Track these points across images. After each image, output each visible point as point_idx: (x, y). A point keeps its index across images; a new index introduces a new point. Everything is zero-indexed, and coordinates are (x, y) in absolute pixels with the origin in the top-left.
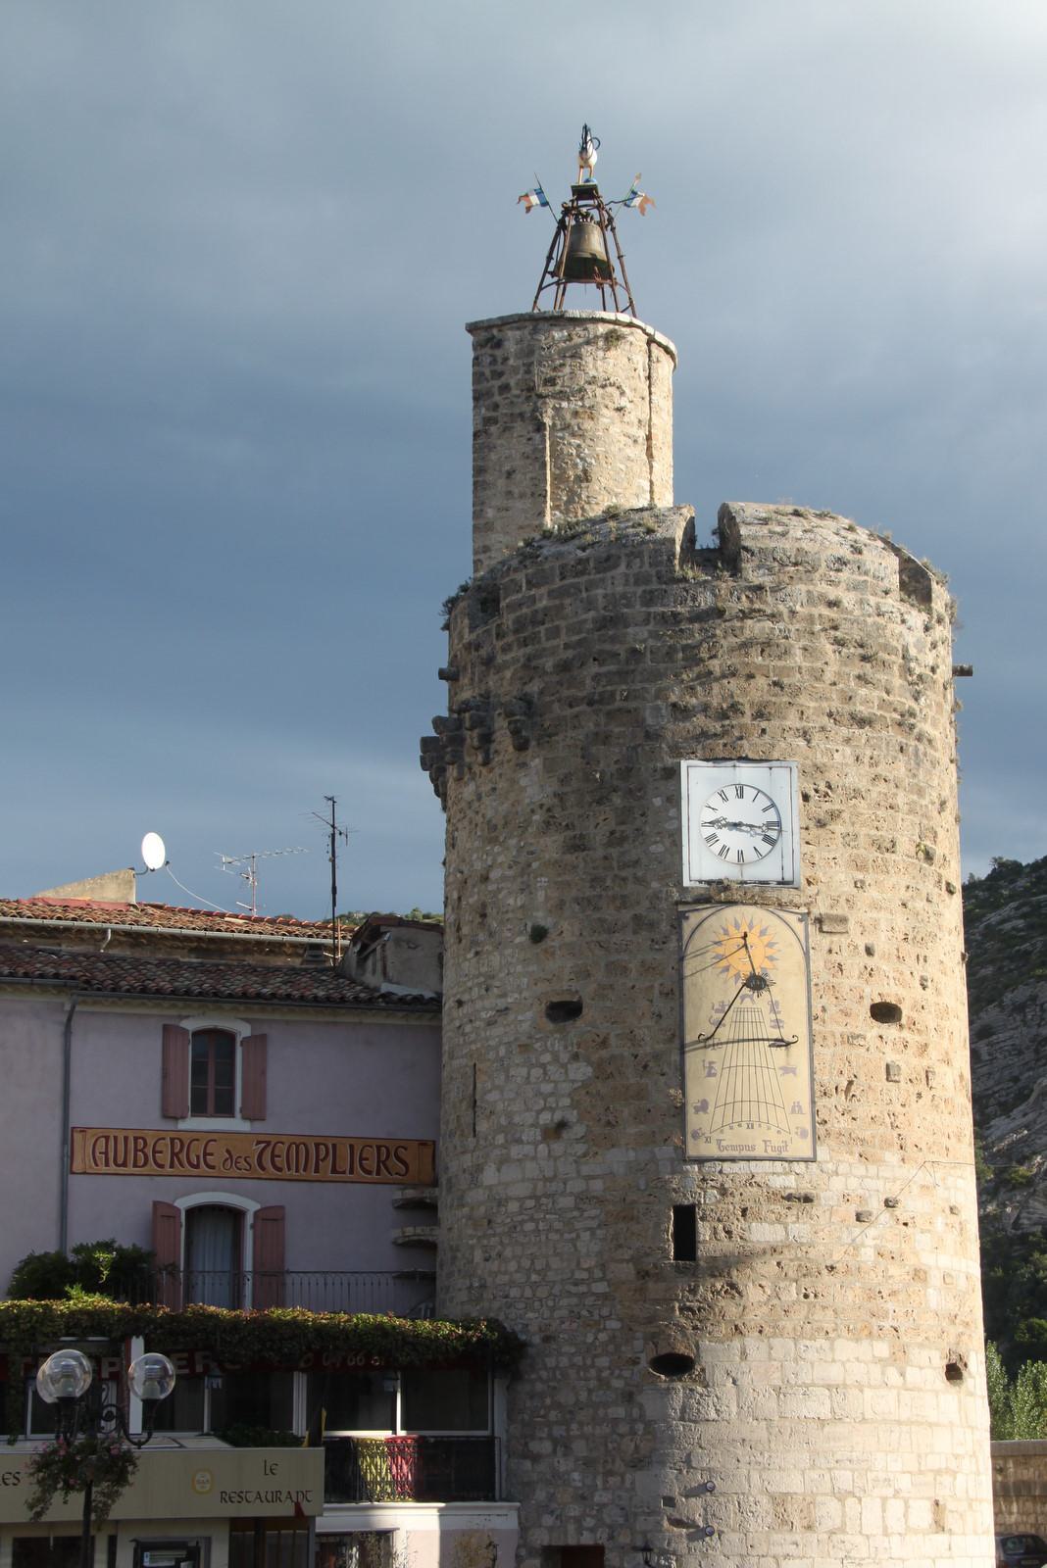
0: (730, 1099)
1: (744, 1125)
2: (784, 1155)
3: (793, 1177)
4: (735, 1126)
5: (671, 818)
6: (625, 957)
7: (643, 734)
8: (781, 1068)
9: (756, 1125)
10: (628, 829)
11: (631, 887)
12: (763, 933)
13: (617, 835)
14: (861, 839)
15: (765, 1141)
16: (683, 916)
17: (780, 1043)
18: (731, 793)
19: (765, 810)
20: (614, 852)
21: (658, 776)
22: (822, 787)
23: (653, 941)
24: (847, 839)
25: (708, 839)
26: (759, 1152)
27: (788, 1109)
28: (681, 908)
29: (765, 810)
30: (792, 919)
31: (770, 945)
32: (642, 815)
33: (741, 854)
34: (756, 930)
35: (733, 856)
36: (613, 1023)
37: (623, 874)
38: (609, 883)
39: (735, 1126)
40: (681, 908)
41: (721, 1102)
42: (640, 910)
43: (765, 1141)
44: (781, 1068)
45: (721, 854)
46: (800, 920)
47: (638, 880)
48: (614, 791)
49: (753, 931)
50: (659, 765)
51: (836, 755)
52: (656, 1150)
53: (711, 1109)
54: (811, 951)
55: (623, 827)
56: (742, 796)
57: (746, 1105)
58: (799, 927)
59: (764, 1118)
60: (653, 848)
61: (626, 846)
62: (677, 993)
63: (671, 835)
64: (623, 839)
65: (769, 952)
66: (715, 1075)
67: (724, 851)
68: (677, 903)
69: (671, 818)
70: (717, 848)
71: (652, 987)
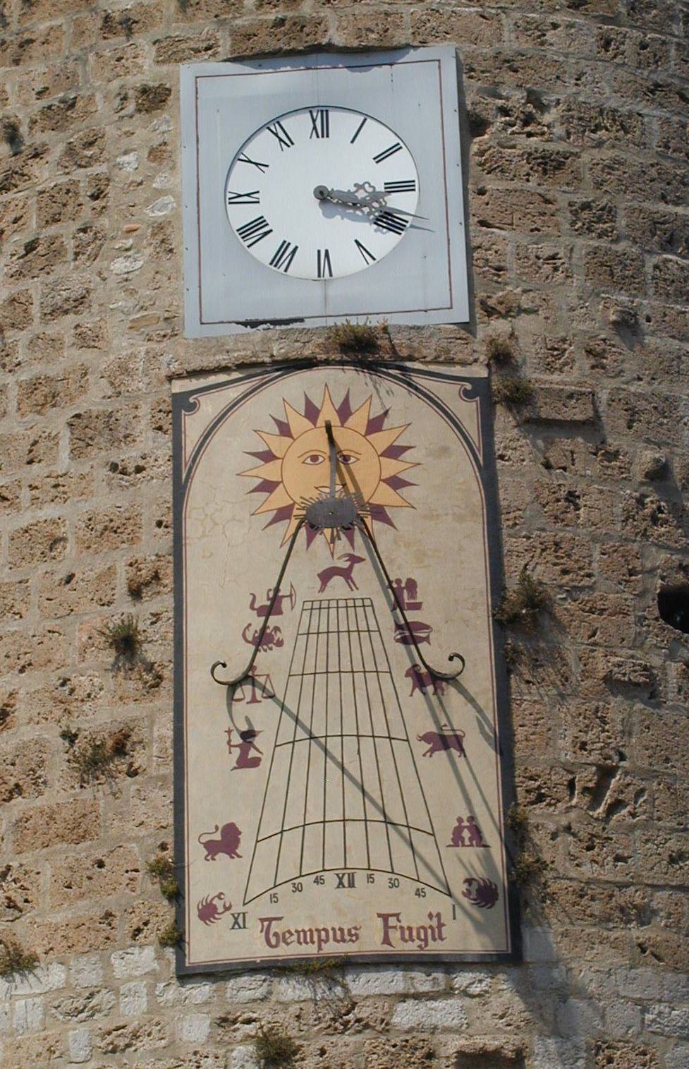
0: (294, 819)
1: (331, 879)
2: (435, 947)
3: (455, 1003)
4: (307, 881)
5: (159, 193)
6: (49, 511)
7: (100, 23)
8: (426, 738)
9: (360, 877)
10: (66, 231)
11: (72, 356)
12: (375, 425)
13: (41, 250)
14: (622, 222)
15: (385, 917)
16: (182, 404)
17: (426, 678)
18: (299, 126)
19: (379, 159)
20: (34, 288)
21: (131, 107)
22: (517, 98)
23: (114, 467)
24: (585, 215)
25: (245, 231)
26: (371, 942)
27: (446, 837)
28: (178, 387)
29: (379, 159)
30: (448, 393)
31: (394, 452)
32: (95, 197)
33: (324, 257)
34: (359, 420)
35: (304, 265)
36: (22, 670)
37: (52, 330)
38: (21, 354)
39: (307, 881)
40: (178, 387)
41: (271, 827)
42: (94, 399)
43: (385, 917)
44: (426, 738)
45: (275, 261)
46: (468, 395)
47: (86, 339)
48: (36, 156)
49: (351, 422)
50: (135, 81)
51: (550, 36)
52: (115, 961)
53: (245, 846)
54: (499, 464)
55: (52, 230)
56: (325, 133)
57: (334, 830)
58: (468, 412)
59: (380, 861)
60: (120, 265)
61: (59, 270)
62: (169, 581)
63: (159, 227)
64: (56, 252)
65: (391, 467)
66: (255, 762)
67: (285, 253)
68: (170, 378)
69: (159, 193)
70: (265, 250)
71: (111, 571)
